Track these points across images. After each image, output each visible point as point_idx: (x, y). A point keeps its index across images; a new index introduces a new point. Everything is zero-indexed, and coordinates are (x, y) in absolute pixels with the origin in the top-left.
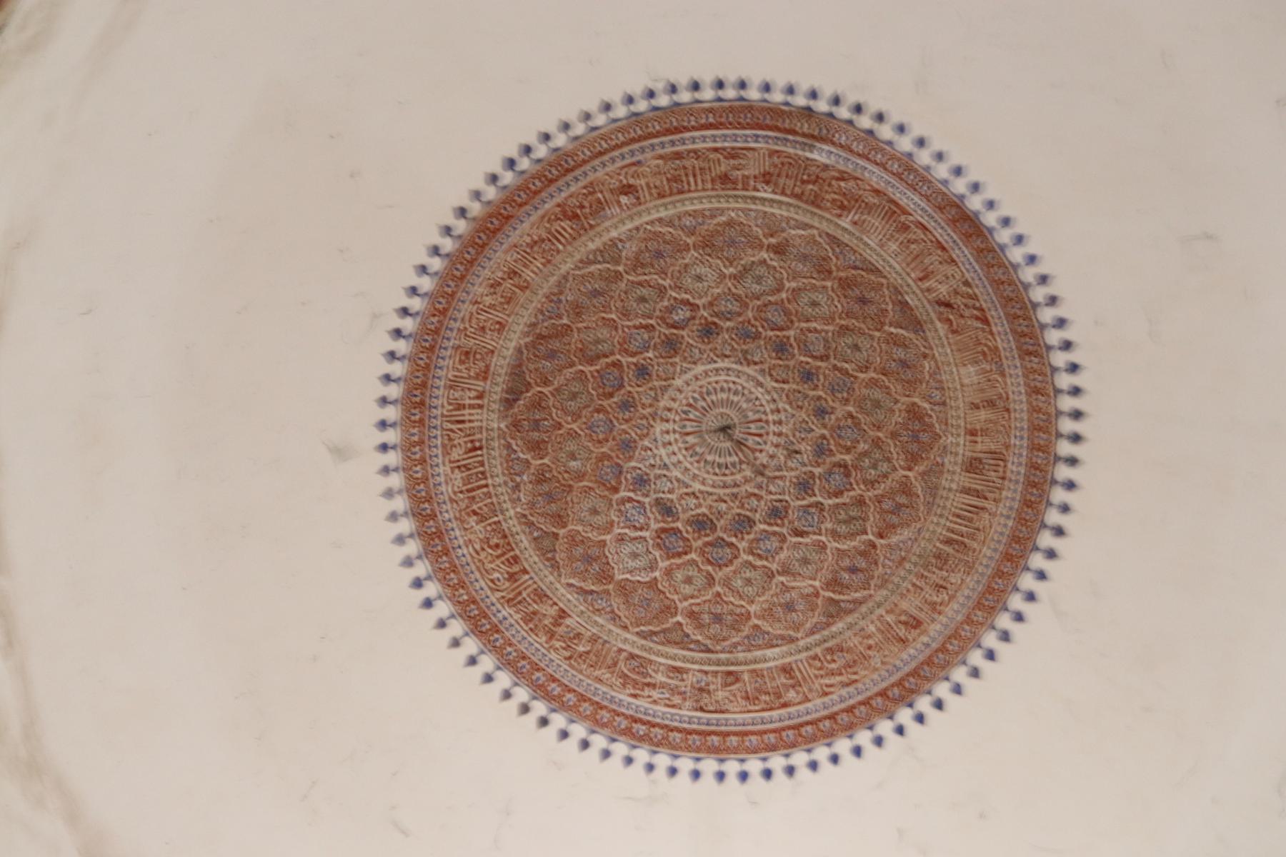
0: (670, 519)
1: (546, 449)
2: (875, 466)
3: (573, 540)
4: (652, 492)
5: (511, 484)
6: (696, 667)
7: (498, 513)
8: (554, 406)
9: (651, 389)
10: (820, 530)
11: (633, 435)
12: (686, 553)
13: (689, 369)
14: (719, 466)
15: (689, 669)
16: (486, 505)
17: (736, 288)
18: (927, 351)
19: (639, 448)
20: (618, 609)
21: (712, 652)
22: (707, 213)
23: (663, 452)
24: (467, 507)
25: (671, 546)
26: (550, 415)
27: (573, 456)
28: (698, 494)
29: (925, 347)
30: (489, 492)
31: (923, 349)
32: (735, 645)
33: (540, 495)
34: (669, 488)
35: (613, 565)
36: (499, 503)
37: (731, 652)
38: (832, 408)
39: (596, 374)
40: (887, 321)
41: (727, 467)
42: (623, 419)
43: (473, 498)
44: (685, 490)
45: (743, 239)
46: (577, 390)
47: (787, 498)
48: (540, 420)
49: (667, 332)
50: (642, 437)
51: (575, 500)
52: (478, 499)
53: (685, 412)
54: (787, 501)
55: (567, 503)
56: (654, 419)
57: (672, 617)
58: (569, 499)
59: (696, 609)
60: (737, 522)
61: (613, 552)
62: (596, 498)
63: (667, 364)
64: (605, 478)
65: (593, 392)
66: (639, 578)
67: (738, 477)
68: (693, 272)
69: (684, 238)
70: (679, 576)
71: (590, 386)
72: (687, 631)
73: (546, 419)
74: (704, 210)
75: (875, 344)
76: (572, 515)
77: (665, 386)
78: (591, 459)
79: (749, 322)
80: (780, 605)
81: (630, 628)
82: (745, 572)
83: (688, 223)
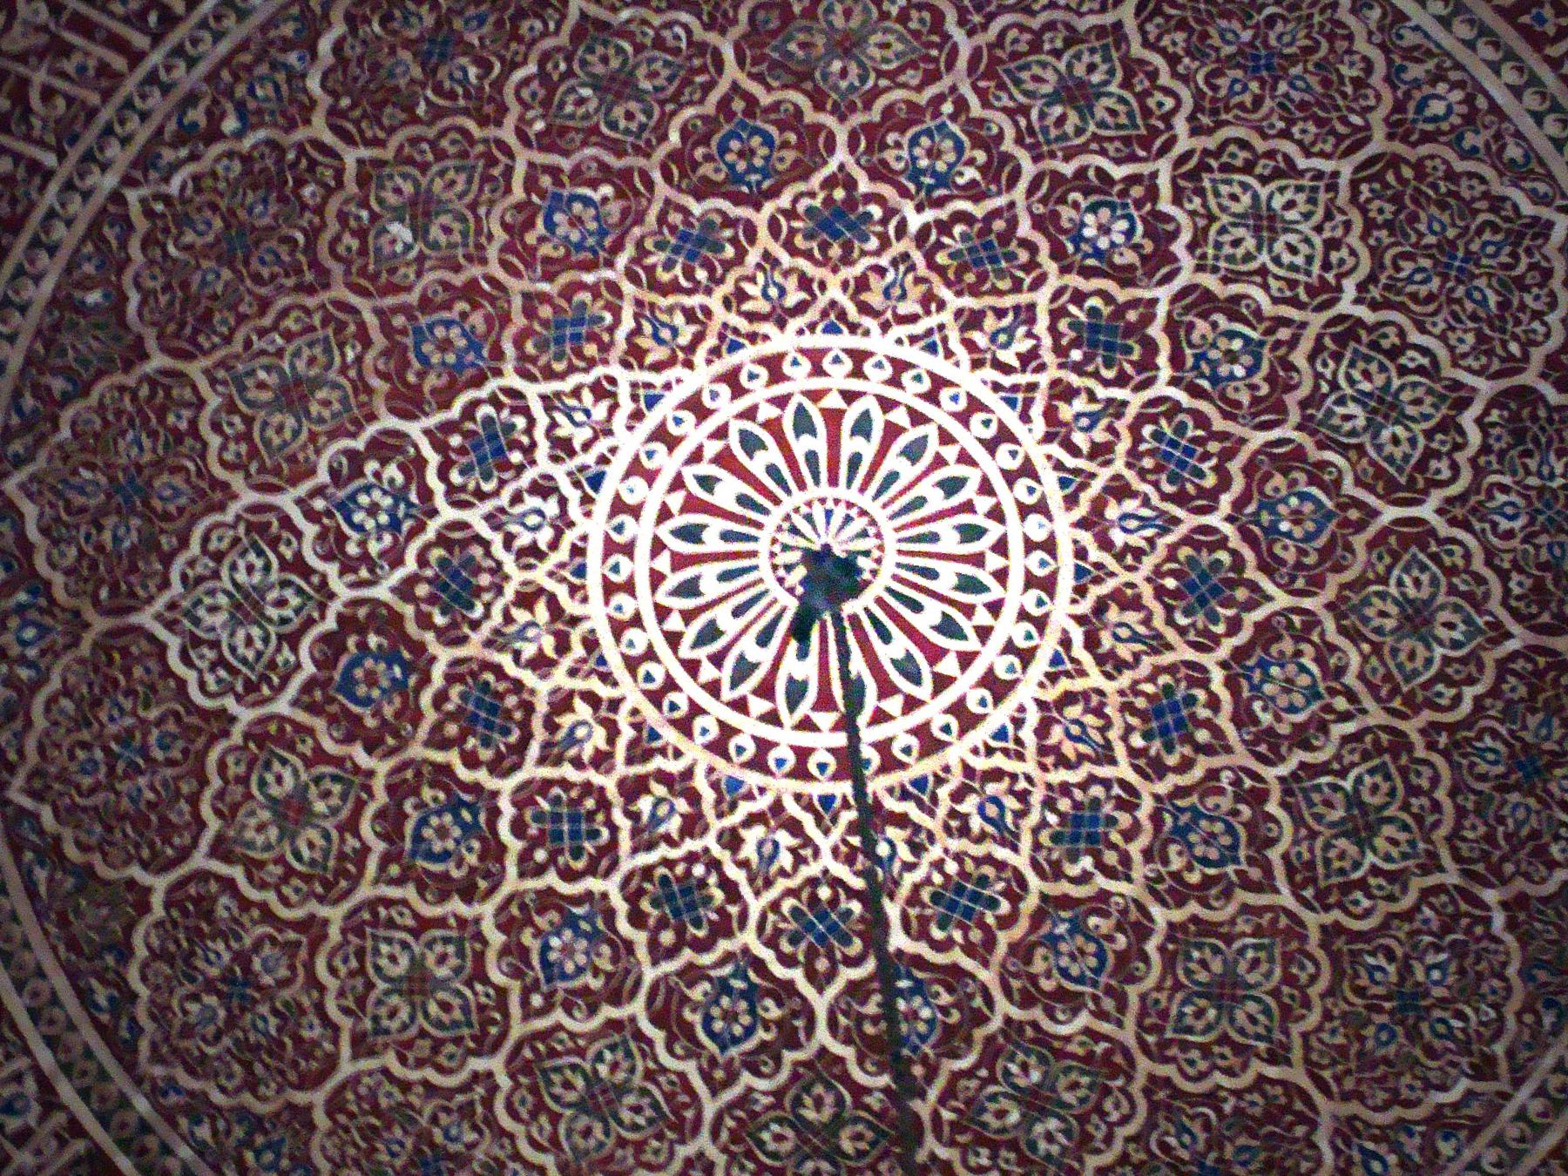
0: (440, 620)
1: (391, 131)
2: (1036, 1102)
3: (161, 414)
4: (488, 506)
5: (197, 115)
6: (45, 1058)
7: (74, 154)
8: (545, 58)
9: (805, 283)
10: (731, 1079)
11: (621, 334)
12: (369, 750)
13: (949, 354)
14: (710, 633)
15: (27, 1051)
16: (70, 100)
17: (1312, 358)
18: (1503, 1067)
19: (589, 378)
20: (52, 701)
21: (130, 1067)
22: (1513, 151)
23: (629, 442)
24: (22, 58)
25: (362, 690)
26: (512, 66)
27: (420, 211)
28: (576, 636)
29: (1510, 1054)
30: (118, 77)
31: (1499, 1049)
32: (198, 1108)
33: (229, 217)
34: (534, 545)
35: (175, 577)
36: (108, 131)
37: (170, 1118)
38: (1126, 860)
39: (738, 105)
40: (1520, 884)
41: (717, 660)
42: (650, 270)
43: (67, 50)
44: (561, 592)
45: (1493, 300)
46: (646, 85)
47: (755, 907)
48: (468, 49)
49: (1025, 229)
50: (634, 356)
51: (290, 323)
52: (69, 66)
53: (802, 416)
54: (744, 916)
55: (264, 305)
56: (715, 352)
57: (145, 866)
58: (283, 302)
59: (224, 906)
60: (574, 819)
61: (213, 545)
62: (343, 370)
63: (919, 280)
64: (427, 348)
65: (674, 137)
66: (191, 676)
67: (718, 710)
68: (1278, 202)
69: (1376, 118)
70: (286, 779)
71: (689, 112)
72: (138, 940)
73: (486, 66)
74: (1518, 135)
75: (1417, 884)
76: (237, 346)
77: (842, 315)
78: (457, 269)
79: (1228, 455)
80: (424, 1137)
81: (19, 781)
82: (442, 959)
83: (1437, 108)
